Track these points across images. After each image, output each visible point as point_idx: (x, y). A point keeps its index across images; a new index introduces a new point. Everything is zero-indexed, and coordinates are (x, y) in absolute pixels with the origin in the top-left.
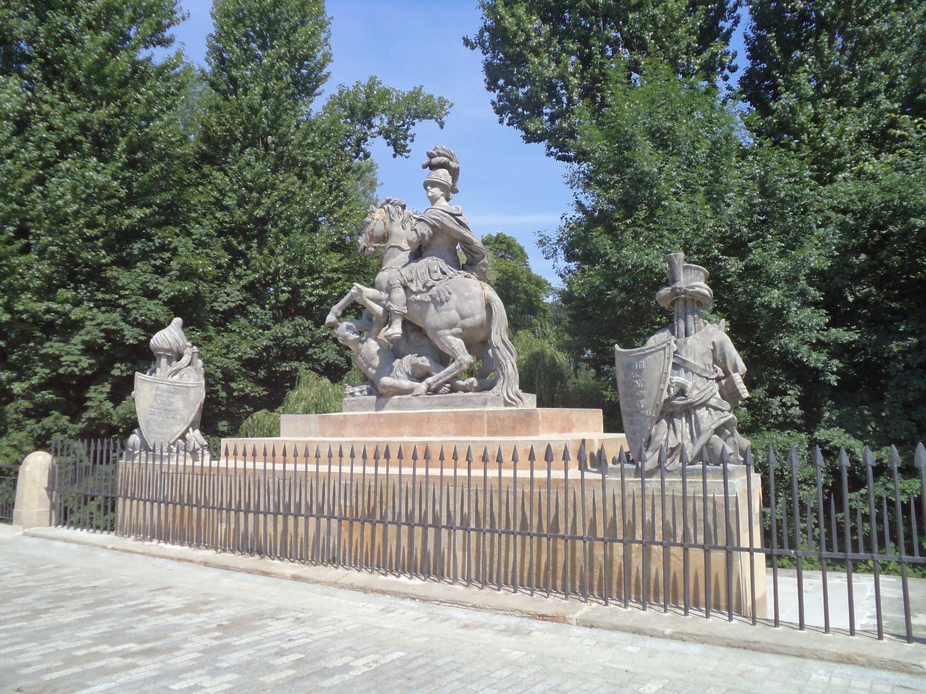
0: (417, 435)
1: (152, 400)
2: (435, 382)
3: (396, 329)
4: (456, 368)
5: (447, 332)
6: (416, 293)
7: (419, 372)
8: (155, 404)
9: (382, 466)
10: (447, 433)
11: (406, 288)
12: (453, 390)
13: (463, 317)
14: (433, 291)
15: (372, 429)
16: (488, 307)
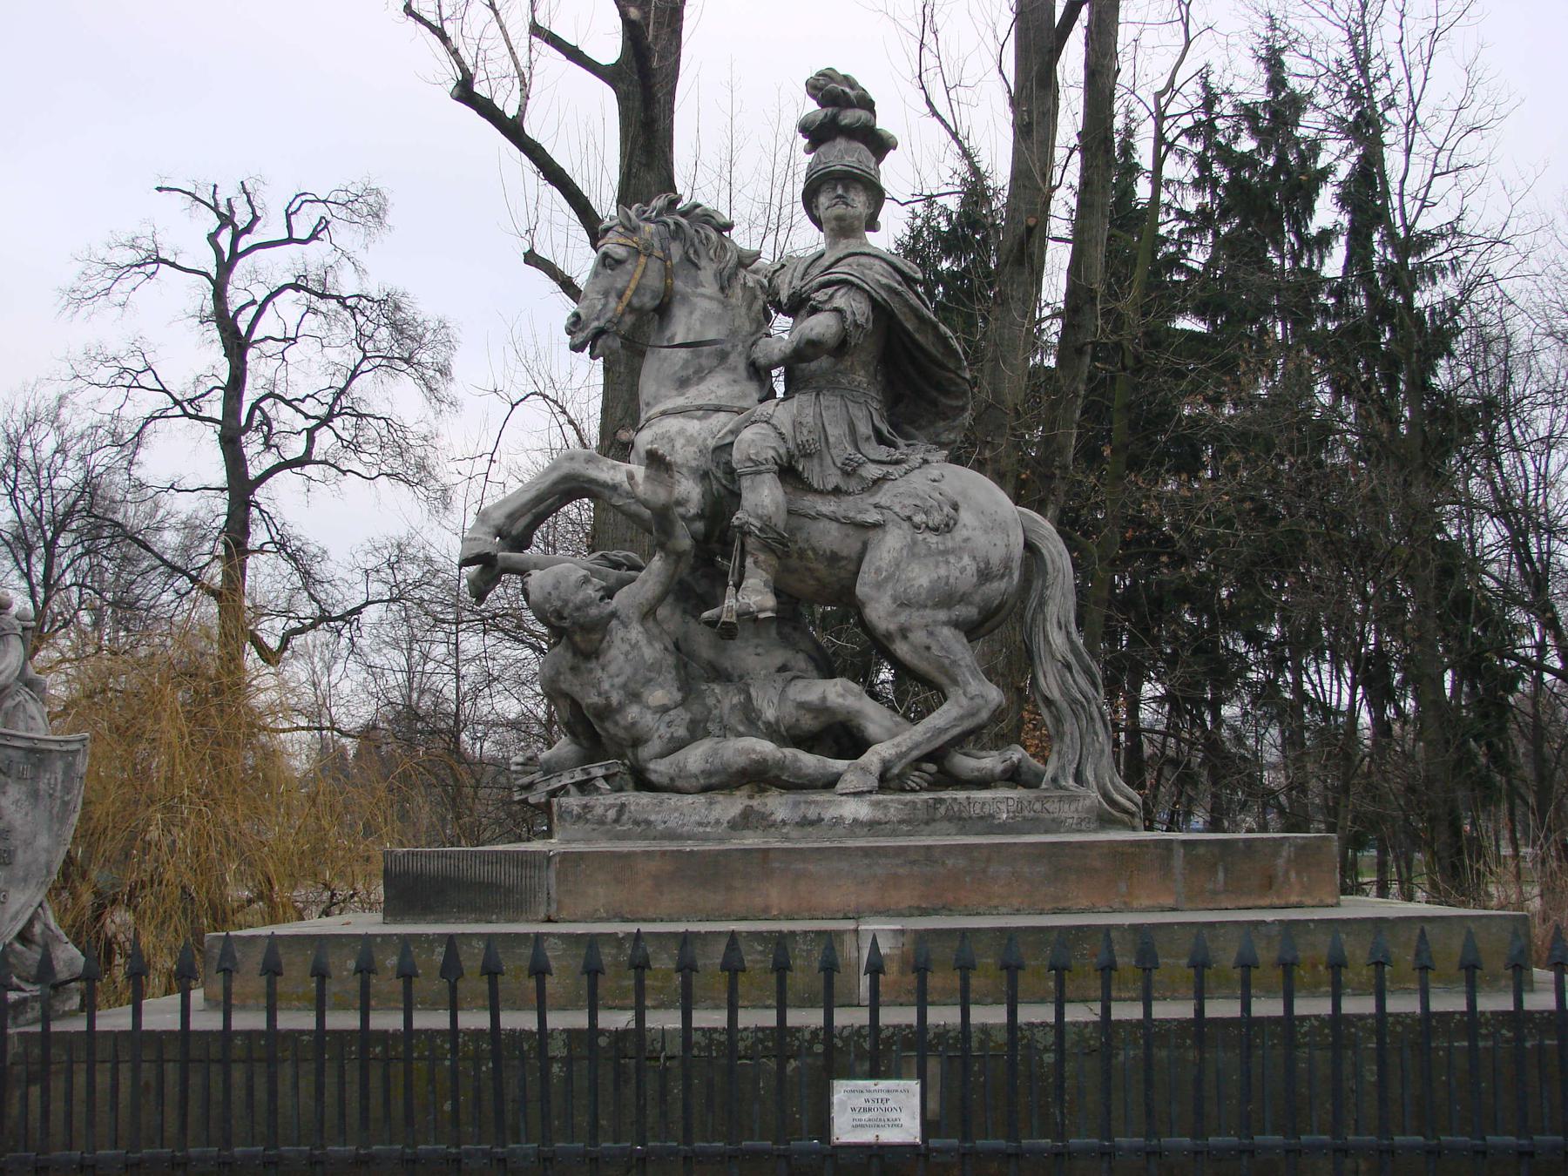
2: (900, 756)
3: (754, 593)
4: (962, 718)
5: (942, 615)
6: (821, 493)
7: (808, 722)
11: (788, 473)
13: (985, 575)
16: (1029, 546)
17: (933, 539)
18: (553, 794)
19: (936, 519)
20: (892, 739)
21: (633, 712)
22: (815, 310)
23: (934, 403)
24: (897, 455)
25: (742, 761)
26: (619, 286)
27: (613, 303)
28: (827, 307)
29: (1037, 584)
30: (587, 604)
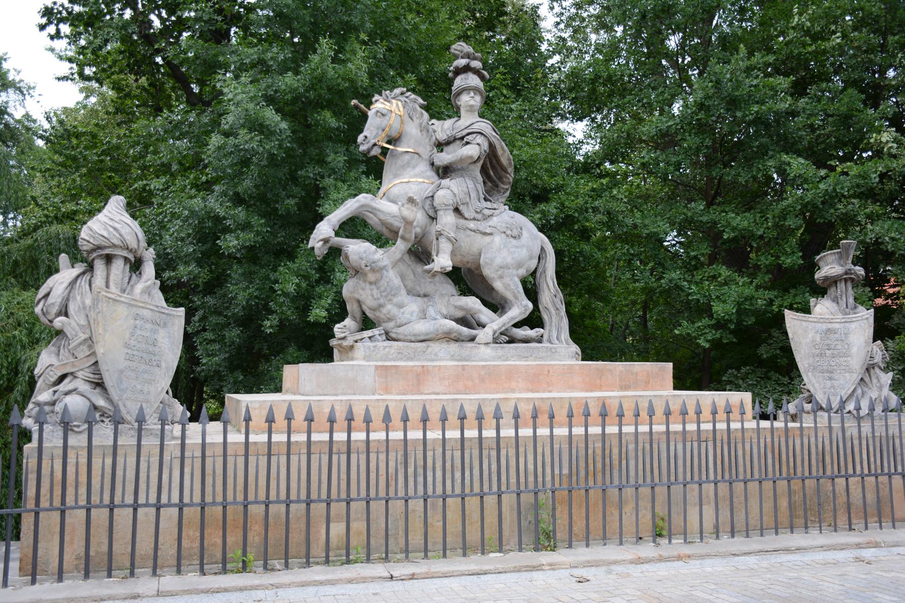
0: (532, 391)
1: (127, 336)
4: (520, 314)
5: (515, 272)
7: (459, 314)
8: (133, 343)
9: (543, 426)
10: (573, 388)
11: (457, 210)
12: (512, 340)
14: (494, 221)
15: (470, 383)
16: (542, 249)
17: (514, 242)
19: (515, 233)
20: (495, 323)
21: (389, 307)
22: (467, 143)
23: (497, 186)
24: (495, 206)
25: (445, 329)
26: (383, 126)
27: (380, 132)
28: (474, 142)
29: (542, 262)
30: (378, 261)
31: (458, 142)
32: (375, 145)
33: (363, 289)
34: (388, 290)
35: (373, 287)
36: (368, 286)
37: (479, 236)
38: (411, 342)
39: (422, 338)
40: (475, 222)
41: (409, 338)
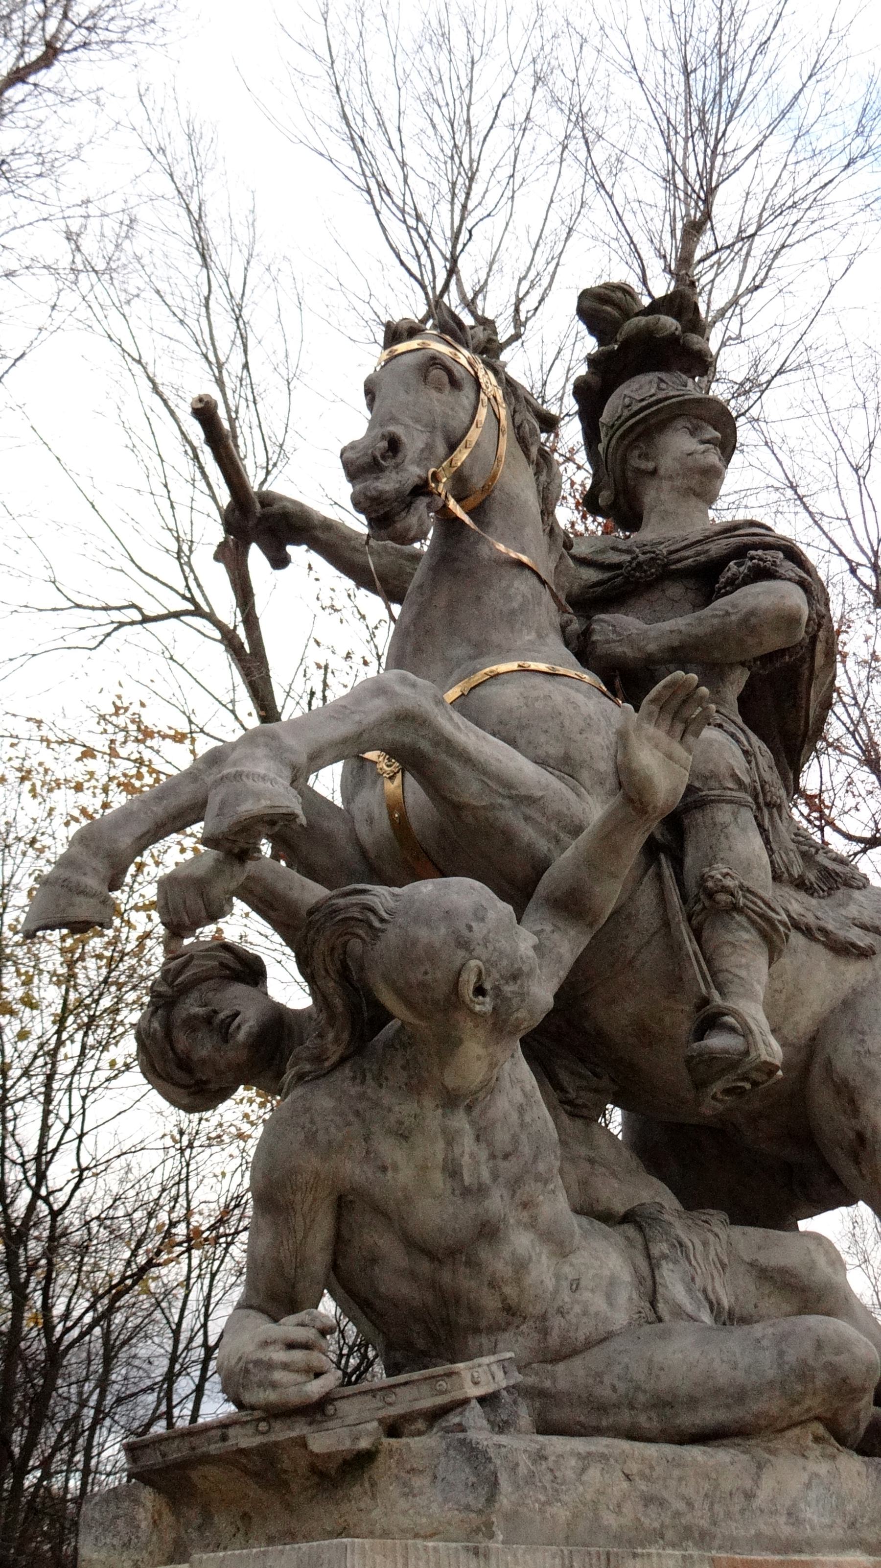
18: (393, 1429)
27: (441, 449)
31: (675, 590)
32: (421, 489)
33: (403, 1135)
34: (526, 1150)
35: (460, 1121)
36: (433, 1118)
37: (821, 956)
38: (634, 1435)
39: (708, 1416)
40: (802, 896)
41: (625, 1418)
